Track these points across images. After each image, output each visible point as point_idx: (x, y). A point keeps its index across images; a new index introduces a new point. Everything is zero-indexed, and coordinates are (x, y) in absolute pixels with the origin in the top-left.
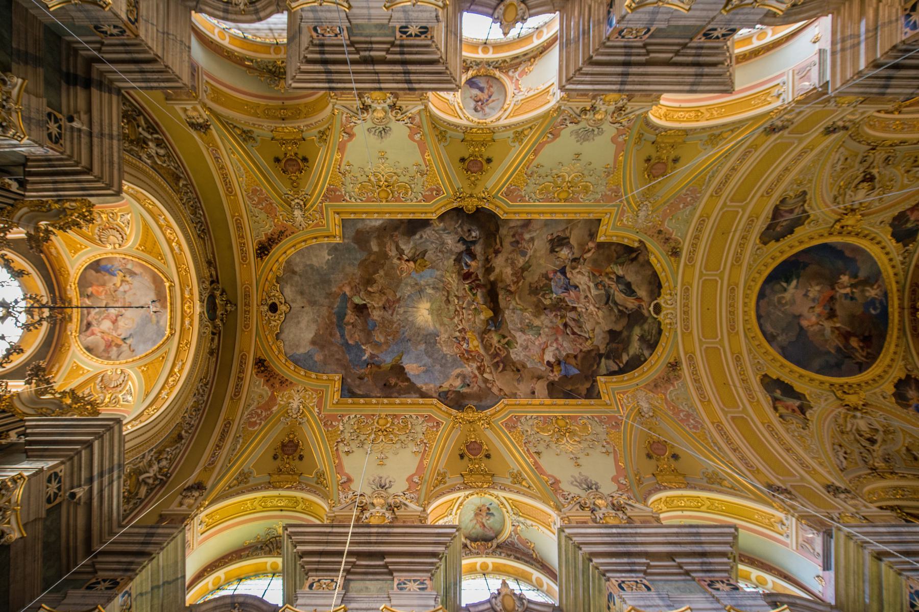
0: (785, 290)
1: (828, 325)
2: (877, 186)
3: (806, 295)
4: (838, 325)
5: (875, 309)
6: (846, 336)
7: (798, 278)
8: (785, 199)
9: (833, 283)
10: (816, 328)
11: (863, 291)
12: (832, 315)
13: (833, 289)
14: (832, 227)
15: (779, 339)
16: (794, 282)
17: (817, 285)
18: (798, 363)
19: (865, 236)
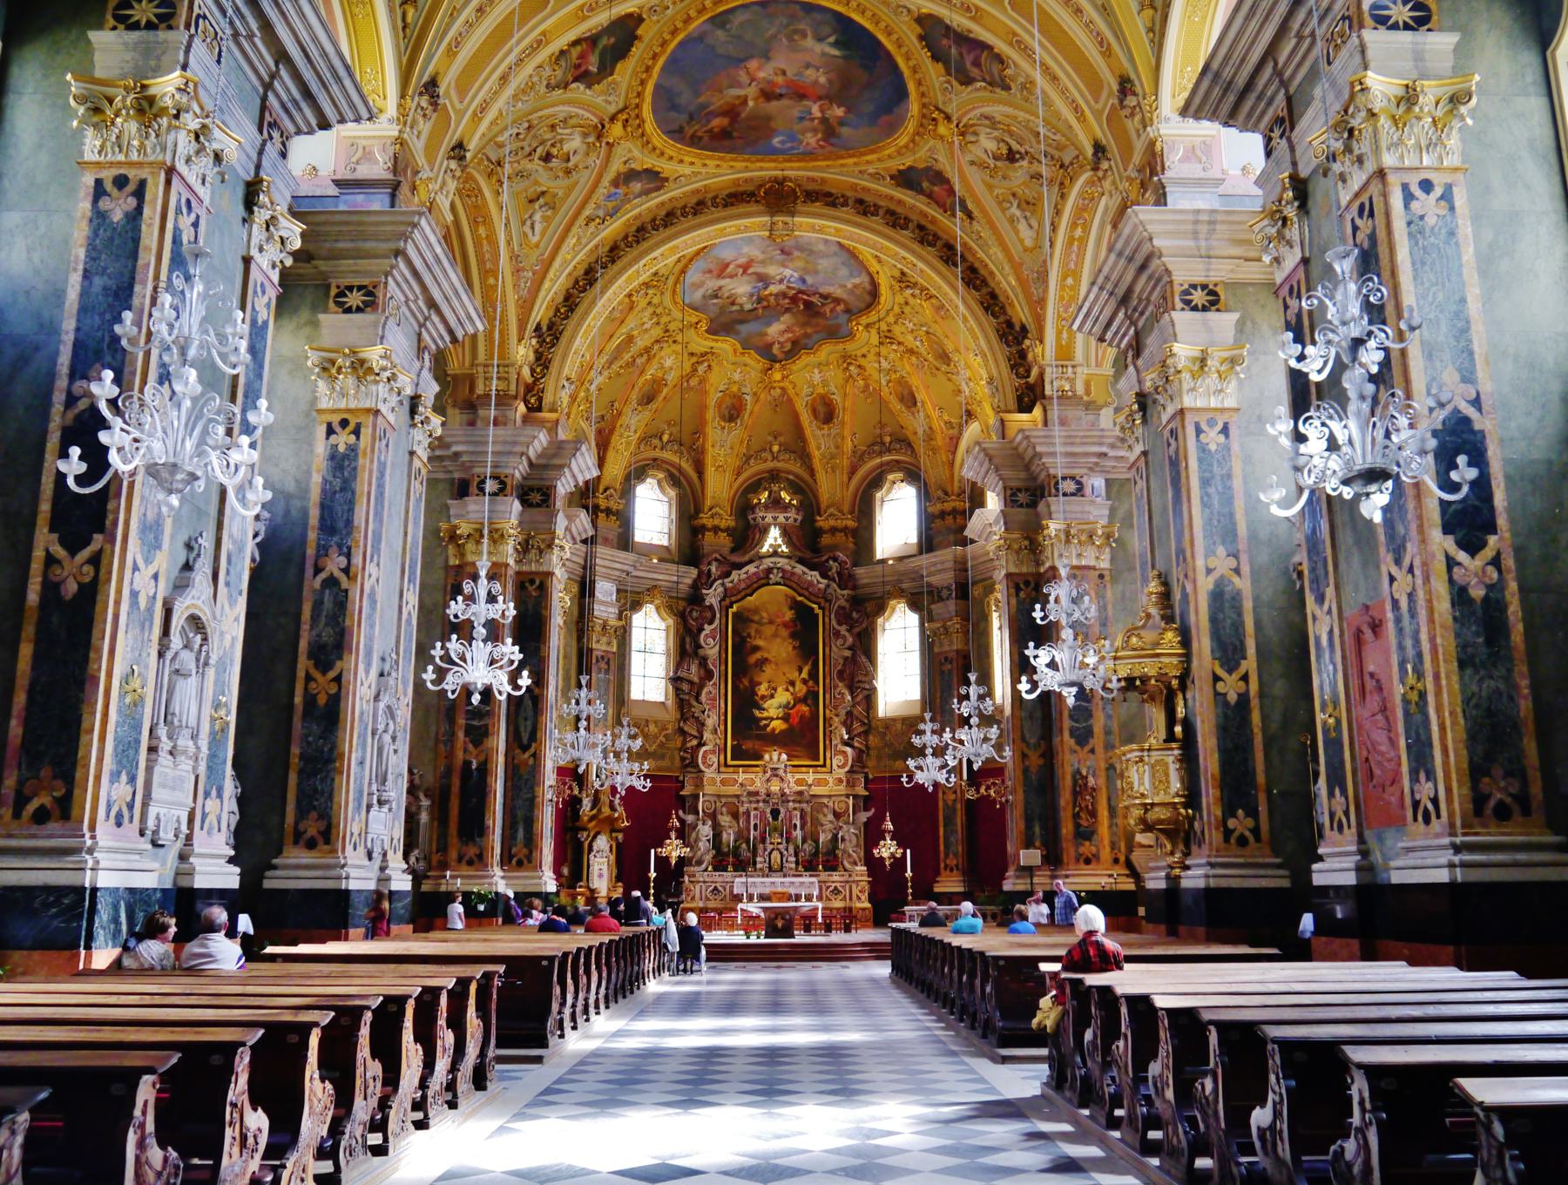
0: (820, 39)
1: (751, 91)
2: (999, 164)
3: (808, 66)
4: (751, 103)
5: (782, 142)
6: (732, 112)
7: (845, 58)
8: (1002, 62)
9: (829, 98)
10: (744, 78)
11: (815, 131)
12: (768, 95)
13: (820, 98)
14: (937, 109)
15: (720, 33)
16: (836, 52)
17: (830, 81)
18: (673, 61)
19: (913, 141)
